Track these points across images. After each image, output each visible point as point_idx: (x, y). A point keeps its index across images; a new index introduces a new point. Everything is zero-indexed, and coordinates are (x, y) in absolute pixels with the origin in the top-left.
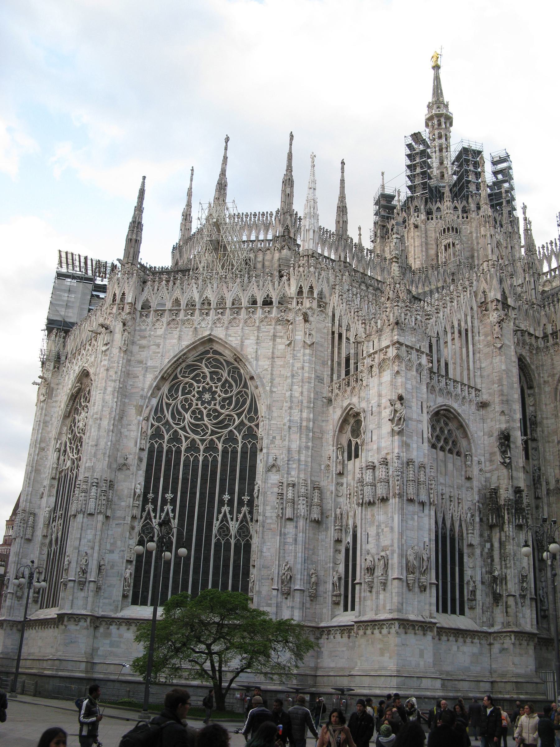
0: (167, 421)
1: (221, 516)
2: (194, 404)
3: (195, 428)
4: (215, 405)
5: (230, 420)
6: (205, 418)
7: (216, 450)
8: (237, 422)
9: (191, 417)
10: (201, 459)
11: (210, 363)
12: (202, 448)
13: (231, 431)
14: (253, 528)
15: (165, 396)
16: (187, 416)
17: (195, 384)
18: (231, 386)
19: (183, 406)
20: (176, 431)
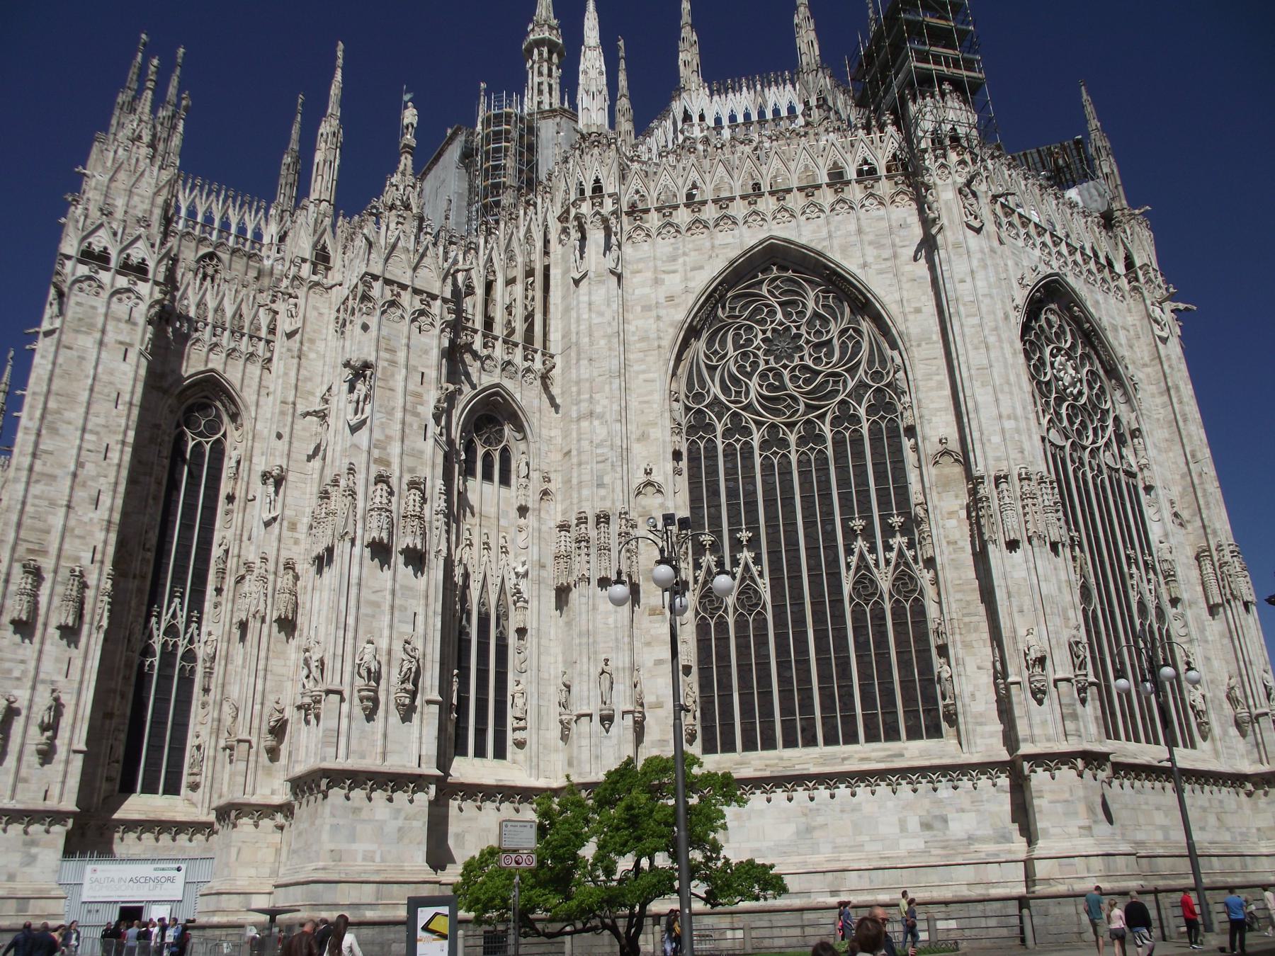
0: (716, 397)
1: (854, 560)
2: (762, 363)
4: (802, 358)
5: (836, 383)
6: (790, 385)
7: (820, 438)
8: (851, 384)
9: (761, 386)
10: (794, 458)
11: (777, 287)
12: (792, 438)
13: (843, 402)
15: (702, 356)
16: (754, 383)
19: (741, 368)
20: (735, 414)
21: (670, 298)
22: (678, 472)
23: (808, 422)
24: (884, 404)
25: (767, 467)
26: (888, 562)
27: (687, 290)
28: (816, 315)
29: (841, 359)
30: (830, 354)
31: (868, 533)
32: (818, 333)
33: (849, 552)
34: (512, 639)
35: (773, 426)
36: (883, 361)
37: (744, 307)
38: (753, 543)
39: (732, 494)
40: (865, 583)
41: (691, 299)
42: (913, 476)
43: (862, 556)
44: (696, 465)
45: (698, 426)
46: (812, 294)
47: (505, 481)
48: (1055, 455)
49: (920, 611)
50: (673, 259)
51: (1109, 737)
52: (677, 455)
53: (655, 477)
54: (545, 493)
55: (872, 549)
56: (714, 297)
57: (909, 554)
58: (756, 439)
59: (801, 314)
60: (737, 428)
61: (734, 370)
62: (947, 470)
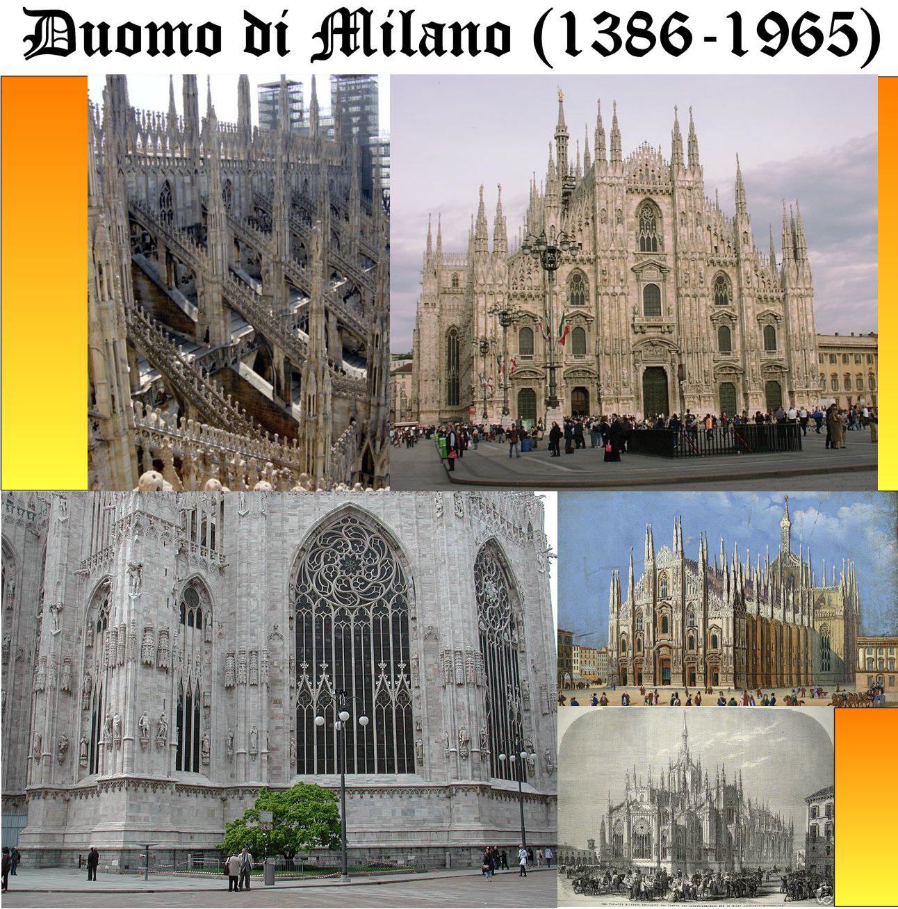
1: (379, 683)
3: (343, 597)
5: (377, 589)
6: (352, 587)
7: (367, 619)
8: (385, 592)
11: (350, 531)
12: (352, 617)
13: (380, 600)
14: (414, 693)
16: (334, 585)
17: (337, 553)
18: (374, 555)
21: (292, 531)
22: (291, 628)
23: (361, 609)
24: (401, 604)
25: (338, 631)
26: (396, 686)
27: (301, 527)
28: (369, 550)
29: (381, 576)
30: (375, 573)
31: (387, 670)
32: (370, 561)
33: (377, 679)
34: (202, 712)
35: (343, 609)
36: (402, 581)
37: (331, 541)
38: (329, 670)
39: (319, 642)
40: (383, 696)
41: (304, 533)
42: (411, 644)
43: (383, 682)
44: (302, 627)
45: (302, 604)
46: (368, 539)
47: (199, 626)
48: (482, 638)
49: (409, 712)
50: (294, 508)
51: (493, 776)
52: (291, 618)
53: (279, 631)
54: (220, 634)
55: (389, 679)
56: (315, 532)
57: (407, 683)
58: (333, 615)
59: (362, 549)
60: (323, 607)
61: (324, 576)
62: (430, 643)
